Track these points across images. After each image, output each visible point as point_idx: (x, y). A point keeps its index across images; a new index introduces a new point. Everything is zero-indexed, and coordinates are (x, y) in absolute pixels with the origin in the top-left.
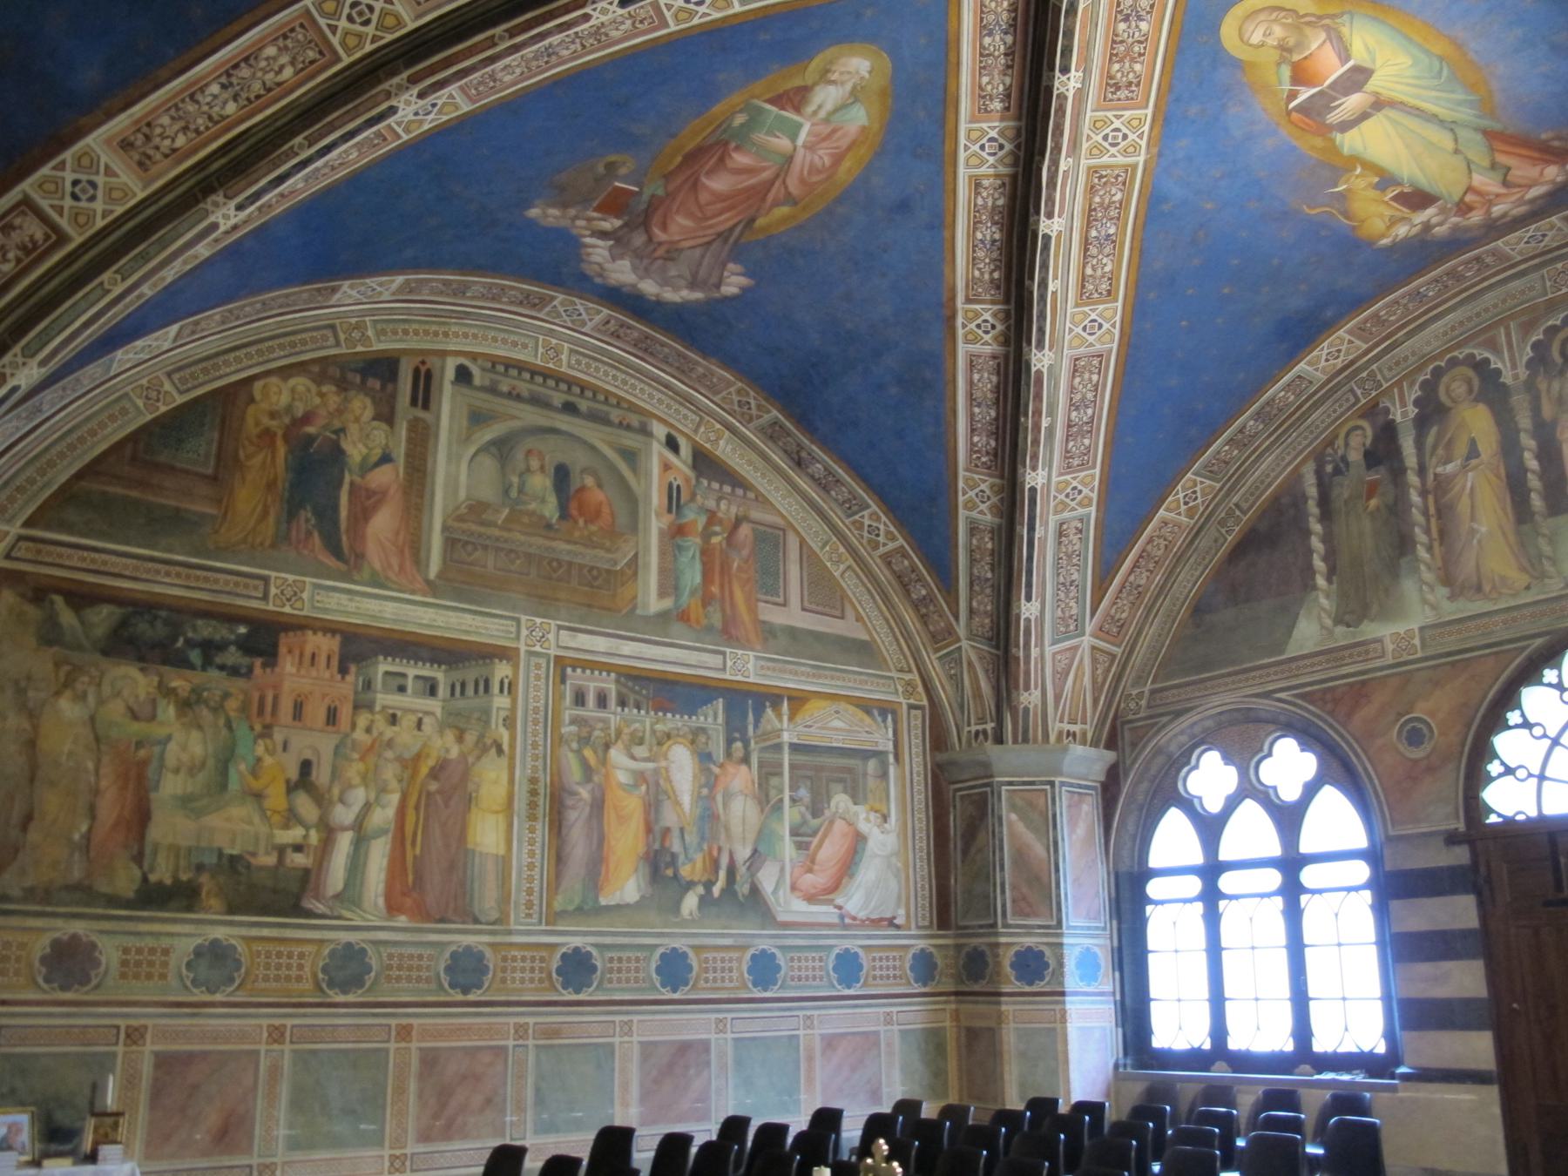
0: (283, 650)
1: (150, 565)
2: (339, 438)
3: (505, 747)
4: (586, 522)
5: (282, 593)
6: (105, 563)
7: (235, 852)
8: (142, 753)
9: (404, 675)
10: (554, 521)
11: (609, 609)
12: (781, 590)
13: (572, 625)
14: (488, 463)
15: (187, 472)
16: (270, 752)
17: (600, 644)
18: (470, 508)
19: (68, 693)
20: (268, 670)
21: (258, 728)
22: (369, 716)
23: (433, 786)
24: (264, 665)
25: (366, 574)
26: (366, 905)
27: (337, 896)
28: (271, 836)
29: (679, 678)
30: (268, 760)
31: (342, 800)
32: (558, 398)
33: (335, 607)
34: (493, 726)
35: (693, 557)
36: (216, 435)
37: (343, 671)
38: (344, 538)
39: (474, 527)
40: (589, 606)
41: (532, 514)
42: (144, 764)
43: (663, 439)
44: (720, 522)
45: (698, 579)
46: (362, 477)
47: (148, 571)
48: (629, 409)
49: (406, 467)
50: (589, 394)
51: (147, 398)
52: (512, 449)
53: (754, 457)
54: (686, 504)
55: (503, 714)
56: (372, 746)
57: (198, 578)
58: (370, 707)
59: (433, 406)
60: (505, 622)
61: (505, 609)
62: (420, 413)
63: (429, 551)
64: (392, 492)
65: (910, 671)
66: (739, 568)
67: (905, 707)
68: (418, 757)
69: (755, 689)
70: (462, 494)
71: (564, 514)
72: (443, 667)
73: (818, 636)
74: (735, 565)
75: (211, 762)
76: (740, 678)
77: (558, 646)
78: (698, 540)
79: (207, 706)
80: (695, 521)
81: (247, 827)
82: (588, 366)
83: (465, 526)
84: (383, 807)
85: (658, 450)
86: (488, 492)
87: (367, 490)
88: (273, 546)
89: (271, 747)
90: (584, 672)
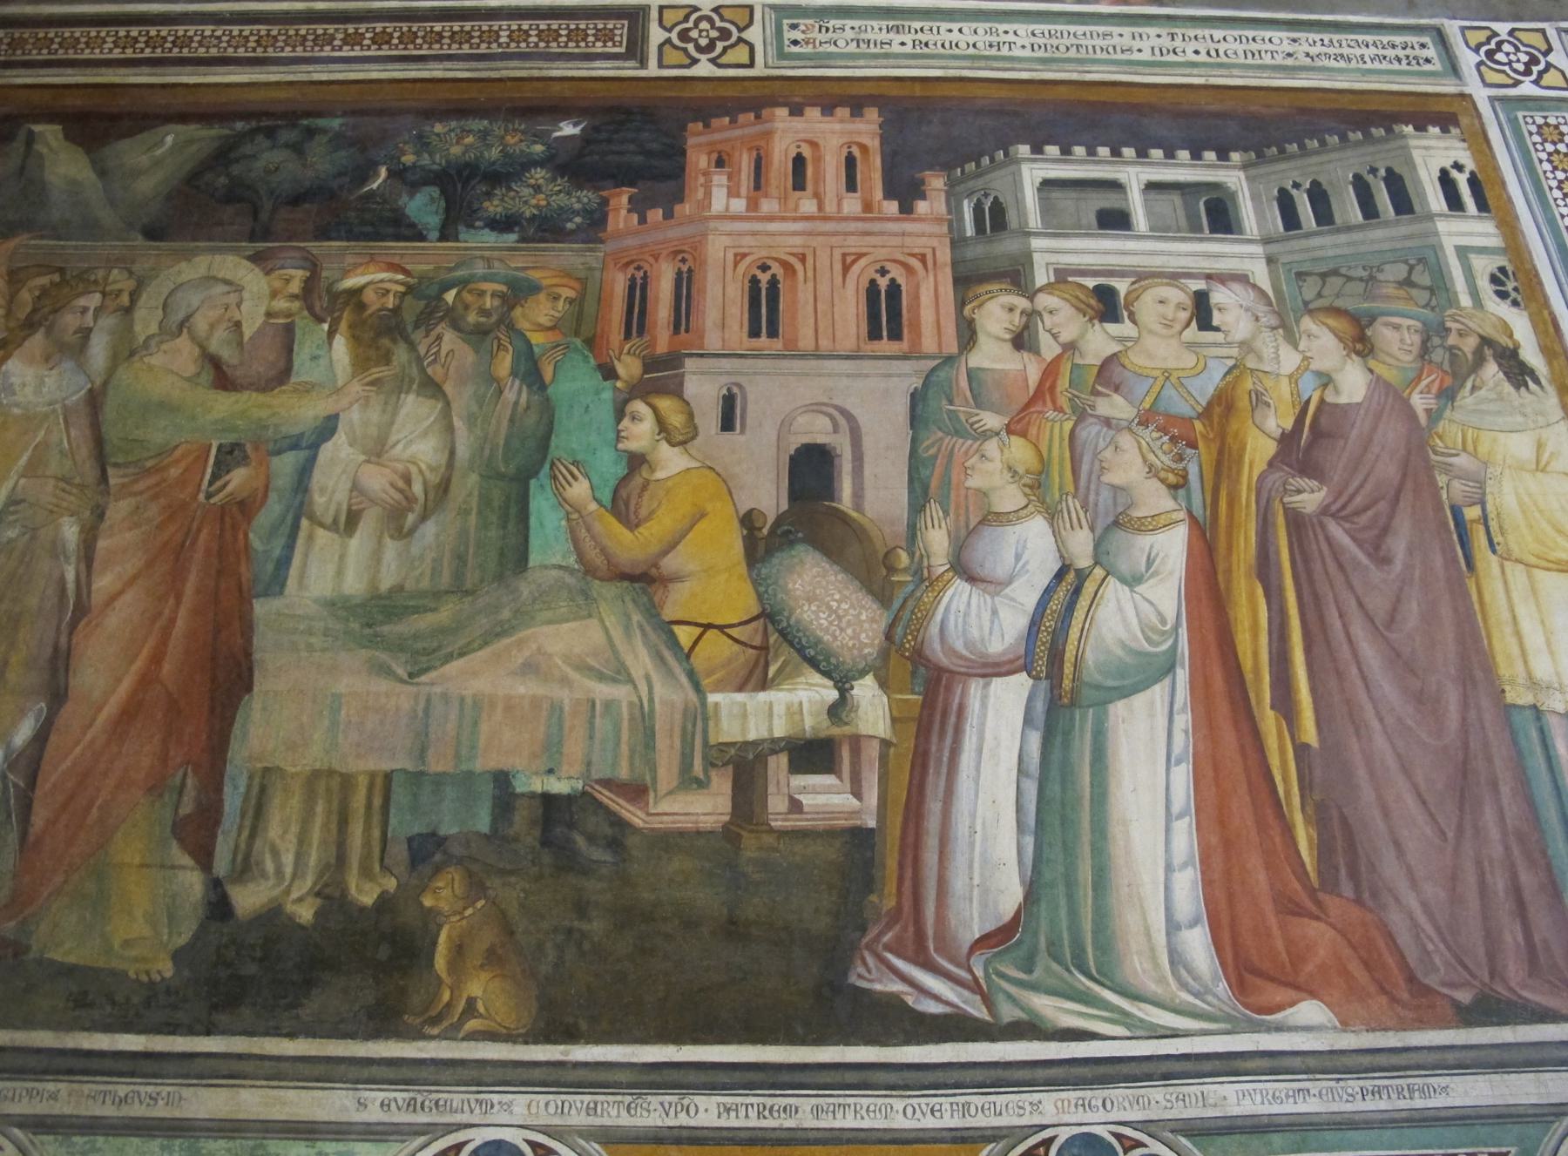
0: (699, 160)
3: (1531, 355)
5: (684, 36)
7: (559, 786)
8: (238, 478)
9: (1115, 186)
16: (683, 439)
19: (38, 340)
20: (656, 215)
21: (629, 368)
22: (1022, 303)
23: (1310, 498)
24: (639, 206)
26: (1138, 967)
27: (998, 938)
28: (698, 717)
30: (671, 462)
31: (962, 568)
34: (1465, 301)
37: (905, 191)
42: (246, 507)
55: (1484, 266)
56: (1045, 390)
58: (1016, 276)
60: (1398, 39)
61: (1392, 12)
68: (1222, 407)
72: (1236, 157)
75: (467, 485)
79: (456, 326)
81: (602, 691)
84: (1132, 581)
89: (676, 420)
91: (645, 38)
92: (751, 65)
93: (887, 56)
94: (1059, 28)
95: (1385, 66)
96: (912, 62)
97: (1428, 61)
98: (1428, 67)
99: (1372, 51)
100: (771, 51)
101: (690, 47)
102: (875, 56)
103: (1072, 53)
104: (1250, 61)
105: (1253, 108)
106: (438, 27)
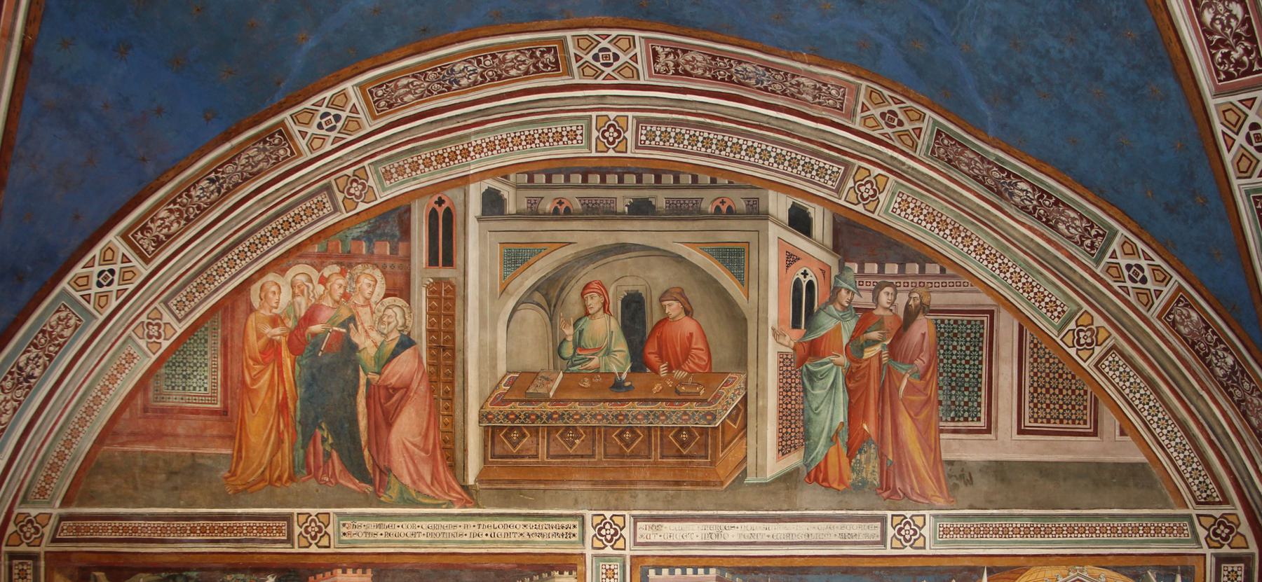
1: (176, 523)
2: (349, 330)
4: (670, 369)
6: (135, 530)
10: (624, 376)
11: (707, 483)
12: (983, 409)
13: (654, 513)
14: (533, 317)
15: (196, 412)
17: (695, 532)
18: (512, 383)
25: (394, 492)
29: (811, 563)
32: (622, 200)
33: (363, 538)
35: (834, 384)
36: (220, 361)
38: (366, 453)
39: (518, 408)
40: (677, 483)
41: (597, 371)
43: (784, 216)
44: (880, 322)
45: (841, 416)
46: (379, 373)
47: (175, 530)
48: (730, 186)
49: (429, 348)
50: (668, 179)
51: (150, 337)
52: (562, 289)
53: (938, 205)
54: (823, 308)
57: (222, 530)
59: (458, 260)
60: (565, 523)
62: (445, 273)
63: (465, 450)
64: (414, 385)
65: (1226, 501)
66: (911, 388)
67: (1210, 562)
69: (934, 563)
70: (502, 368)
71: (639, 362)
73: (1044, 470)
74: (905, 382)
76: (909, 551)
77: (636, 544)
78: (843, 359)
80: (838, 328)
82: (665, 136)
83: (507, 408)
85: (775, 232)
86: (534, 357)
87: (386, 388)
88: (291, 478)
90: (672, 573)
91: (293, 531)
92: (329, 547)
93: (376, 541)
94: (438, 523)
95: (557, 539)
96: (384, 545)
97: (574, 535)
98: (573, 539)
99: (554, 530)
100: (336, 540)
101: (308, 536)
102: (372, 542)
103: (441, 538)
104: (506, 539)
105: (502, 565)
106: (222, 523)
